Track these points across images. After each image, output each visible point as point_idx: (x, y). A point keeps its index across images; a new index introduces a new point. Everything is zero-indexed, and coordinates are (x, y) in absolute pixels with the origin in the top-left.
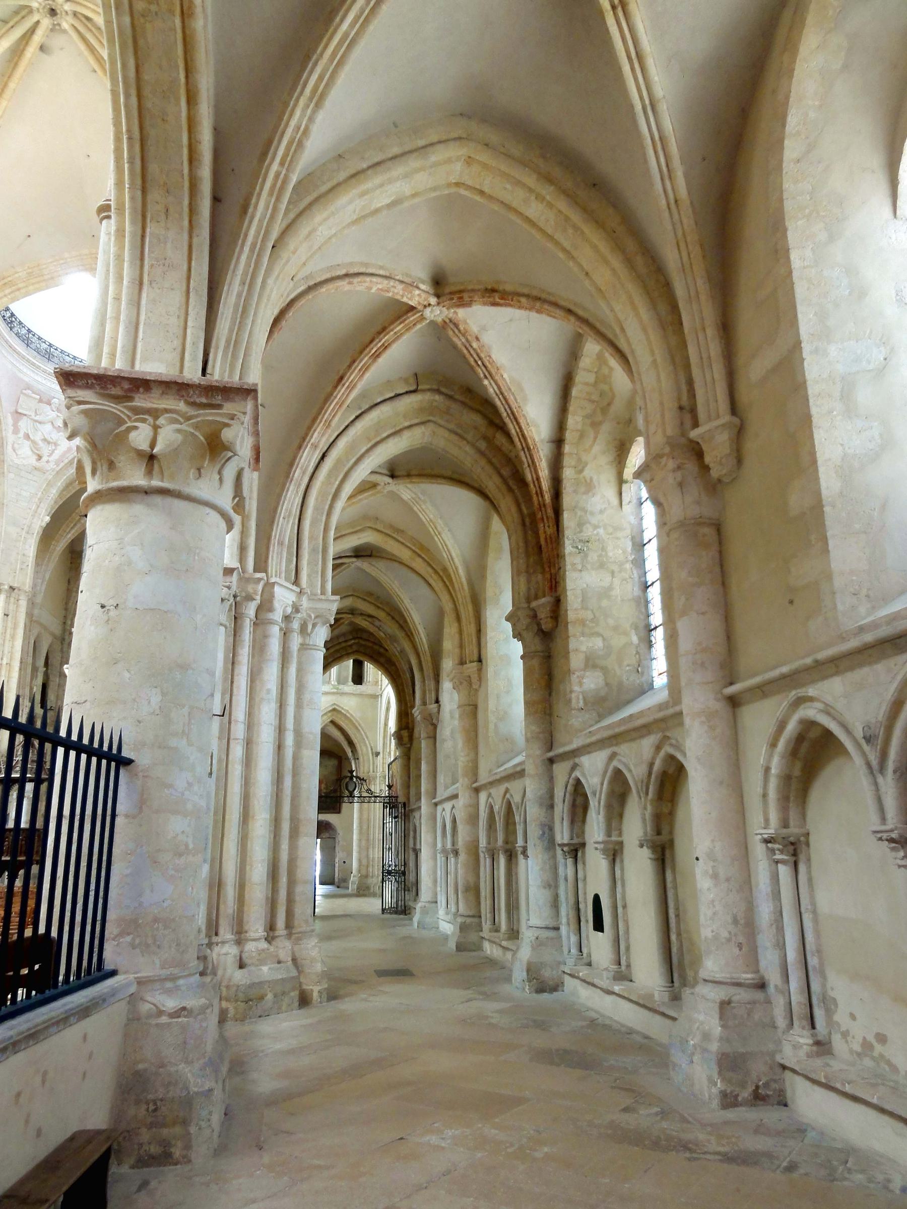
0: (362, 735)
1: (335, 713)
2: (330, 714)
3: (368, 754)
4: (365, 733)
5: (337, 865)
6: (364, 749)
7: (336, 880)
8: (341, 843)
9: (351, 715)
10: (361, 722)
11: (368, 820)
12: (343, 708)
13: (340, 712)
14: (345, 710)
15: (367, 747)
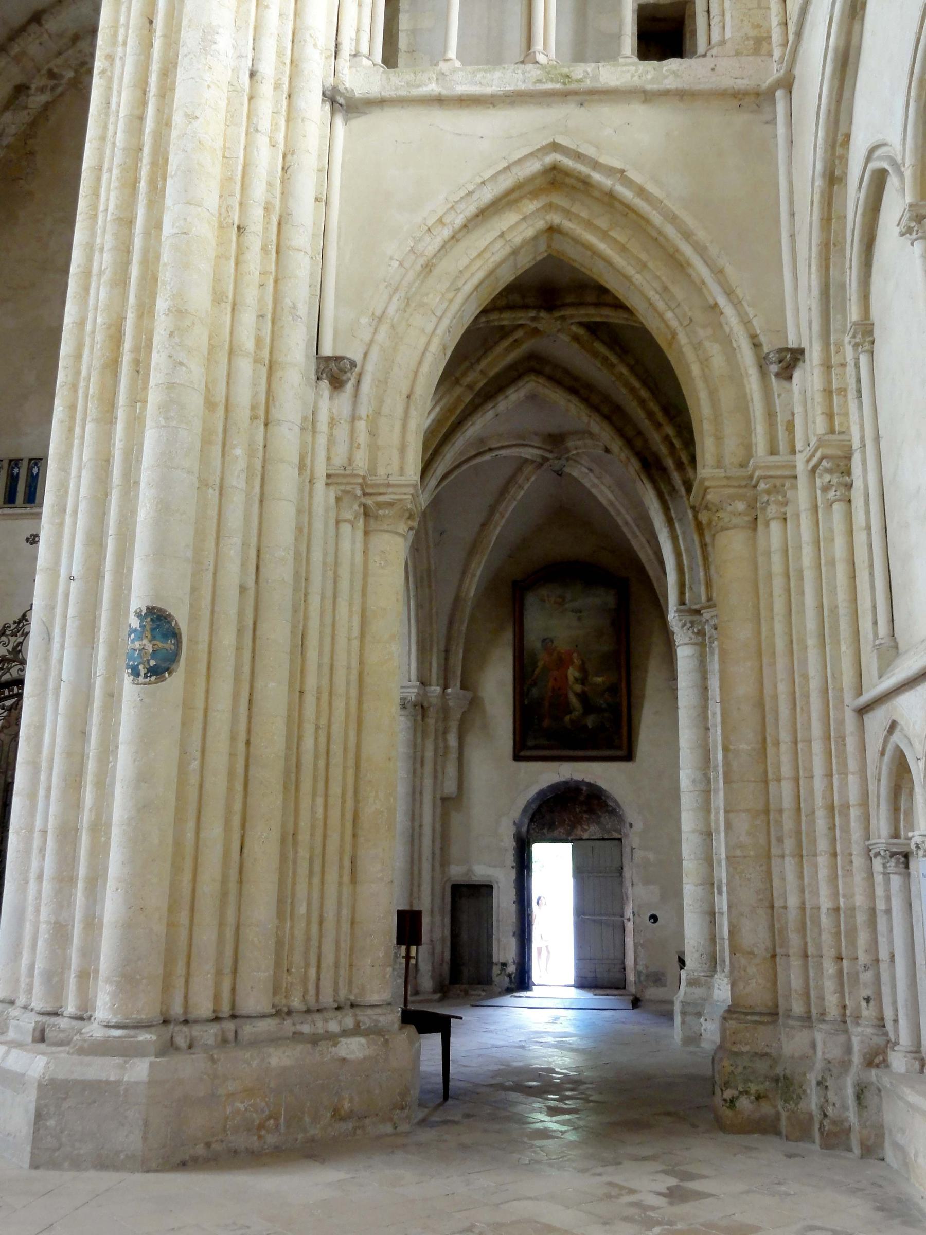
0: (698, 288)
1: (558, 199)
2: (531, 206)
3: (736, 377)
4: (719, 273)
5: (629, 926)
6: (718, 362)
7: (631, 977)
8: (638, 854)
9: (641, 192)
10: (691, 222)
11: (760, 704)
12: (596, 165)
13: (585, 184)
14: (610, 171)
15: (730, 352)
